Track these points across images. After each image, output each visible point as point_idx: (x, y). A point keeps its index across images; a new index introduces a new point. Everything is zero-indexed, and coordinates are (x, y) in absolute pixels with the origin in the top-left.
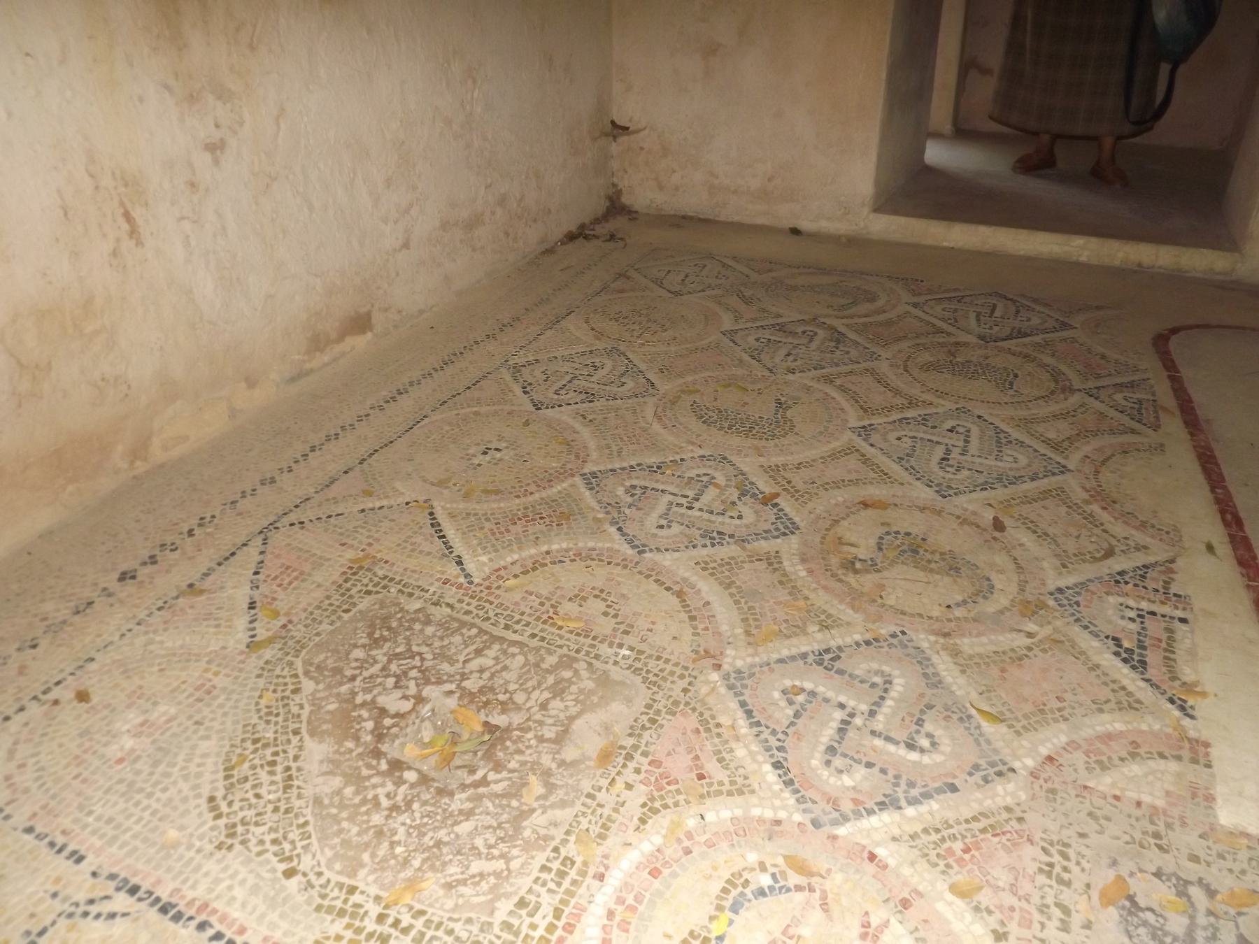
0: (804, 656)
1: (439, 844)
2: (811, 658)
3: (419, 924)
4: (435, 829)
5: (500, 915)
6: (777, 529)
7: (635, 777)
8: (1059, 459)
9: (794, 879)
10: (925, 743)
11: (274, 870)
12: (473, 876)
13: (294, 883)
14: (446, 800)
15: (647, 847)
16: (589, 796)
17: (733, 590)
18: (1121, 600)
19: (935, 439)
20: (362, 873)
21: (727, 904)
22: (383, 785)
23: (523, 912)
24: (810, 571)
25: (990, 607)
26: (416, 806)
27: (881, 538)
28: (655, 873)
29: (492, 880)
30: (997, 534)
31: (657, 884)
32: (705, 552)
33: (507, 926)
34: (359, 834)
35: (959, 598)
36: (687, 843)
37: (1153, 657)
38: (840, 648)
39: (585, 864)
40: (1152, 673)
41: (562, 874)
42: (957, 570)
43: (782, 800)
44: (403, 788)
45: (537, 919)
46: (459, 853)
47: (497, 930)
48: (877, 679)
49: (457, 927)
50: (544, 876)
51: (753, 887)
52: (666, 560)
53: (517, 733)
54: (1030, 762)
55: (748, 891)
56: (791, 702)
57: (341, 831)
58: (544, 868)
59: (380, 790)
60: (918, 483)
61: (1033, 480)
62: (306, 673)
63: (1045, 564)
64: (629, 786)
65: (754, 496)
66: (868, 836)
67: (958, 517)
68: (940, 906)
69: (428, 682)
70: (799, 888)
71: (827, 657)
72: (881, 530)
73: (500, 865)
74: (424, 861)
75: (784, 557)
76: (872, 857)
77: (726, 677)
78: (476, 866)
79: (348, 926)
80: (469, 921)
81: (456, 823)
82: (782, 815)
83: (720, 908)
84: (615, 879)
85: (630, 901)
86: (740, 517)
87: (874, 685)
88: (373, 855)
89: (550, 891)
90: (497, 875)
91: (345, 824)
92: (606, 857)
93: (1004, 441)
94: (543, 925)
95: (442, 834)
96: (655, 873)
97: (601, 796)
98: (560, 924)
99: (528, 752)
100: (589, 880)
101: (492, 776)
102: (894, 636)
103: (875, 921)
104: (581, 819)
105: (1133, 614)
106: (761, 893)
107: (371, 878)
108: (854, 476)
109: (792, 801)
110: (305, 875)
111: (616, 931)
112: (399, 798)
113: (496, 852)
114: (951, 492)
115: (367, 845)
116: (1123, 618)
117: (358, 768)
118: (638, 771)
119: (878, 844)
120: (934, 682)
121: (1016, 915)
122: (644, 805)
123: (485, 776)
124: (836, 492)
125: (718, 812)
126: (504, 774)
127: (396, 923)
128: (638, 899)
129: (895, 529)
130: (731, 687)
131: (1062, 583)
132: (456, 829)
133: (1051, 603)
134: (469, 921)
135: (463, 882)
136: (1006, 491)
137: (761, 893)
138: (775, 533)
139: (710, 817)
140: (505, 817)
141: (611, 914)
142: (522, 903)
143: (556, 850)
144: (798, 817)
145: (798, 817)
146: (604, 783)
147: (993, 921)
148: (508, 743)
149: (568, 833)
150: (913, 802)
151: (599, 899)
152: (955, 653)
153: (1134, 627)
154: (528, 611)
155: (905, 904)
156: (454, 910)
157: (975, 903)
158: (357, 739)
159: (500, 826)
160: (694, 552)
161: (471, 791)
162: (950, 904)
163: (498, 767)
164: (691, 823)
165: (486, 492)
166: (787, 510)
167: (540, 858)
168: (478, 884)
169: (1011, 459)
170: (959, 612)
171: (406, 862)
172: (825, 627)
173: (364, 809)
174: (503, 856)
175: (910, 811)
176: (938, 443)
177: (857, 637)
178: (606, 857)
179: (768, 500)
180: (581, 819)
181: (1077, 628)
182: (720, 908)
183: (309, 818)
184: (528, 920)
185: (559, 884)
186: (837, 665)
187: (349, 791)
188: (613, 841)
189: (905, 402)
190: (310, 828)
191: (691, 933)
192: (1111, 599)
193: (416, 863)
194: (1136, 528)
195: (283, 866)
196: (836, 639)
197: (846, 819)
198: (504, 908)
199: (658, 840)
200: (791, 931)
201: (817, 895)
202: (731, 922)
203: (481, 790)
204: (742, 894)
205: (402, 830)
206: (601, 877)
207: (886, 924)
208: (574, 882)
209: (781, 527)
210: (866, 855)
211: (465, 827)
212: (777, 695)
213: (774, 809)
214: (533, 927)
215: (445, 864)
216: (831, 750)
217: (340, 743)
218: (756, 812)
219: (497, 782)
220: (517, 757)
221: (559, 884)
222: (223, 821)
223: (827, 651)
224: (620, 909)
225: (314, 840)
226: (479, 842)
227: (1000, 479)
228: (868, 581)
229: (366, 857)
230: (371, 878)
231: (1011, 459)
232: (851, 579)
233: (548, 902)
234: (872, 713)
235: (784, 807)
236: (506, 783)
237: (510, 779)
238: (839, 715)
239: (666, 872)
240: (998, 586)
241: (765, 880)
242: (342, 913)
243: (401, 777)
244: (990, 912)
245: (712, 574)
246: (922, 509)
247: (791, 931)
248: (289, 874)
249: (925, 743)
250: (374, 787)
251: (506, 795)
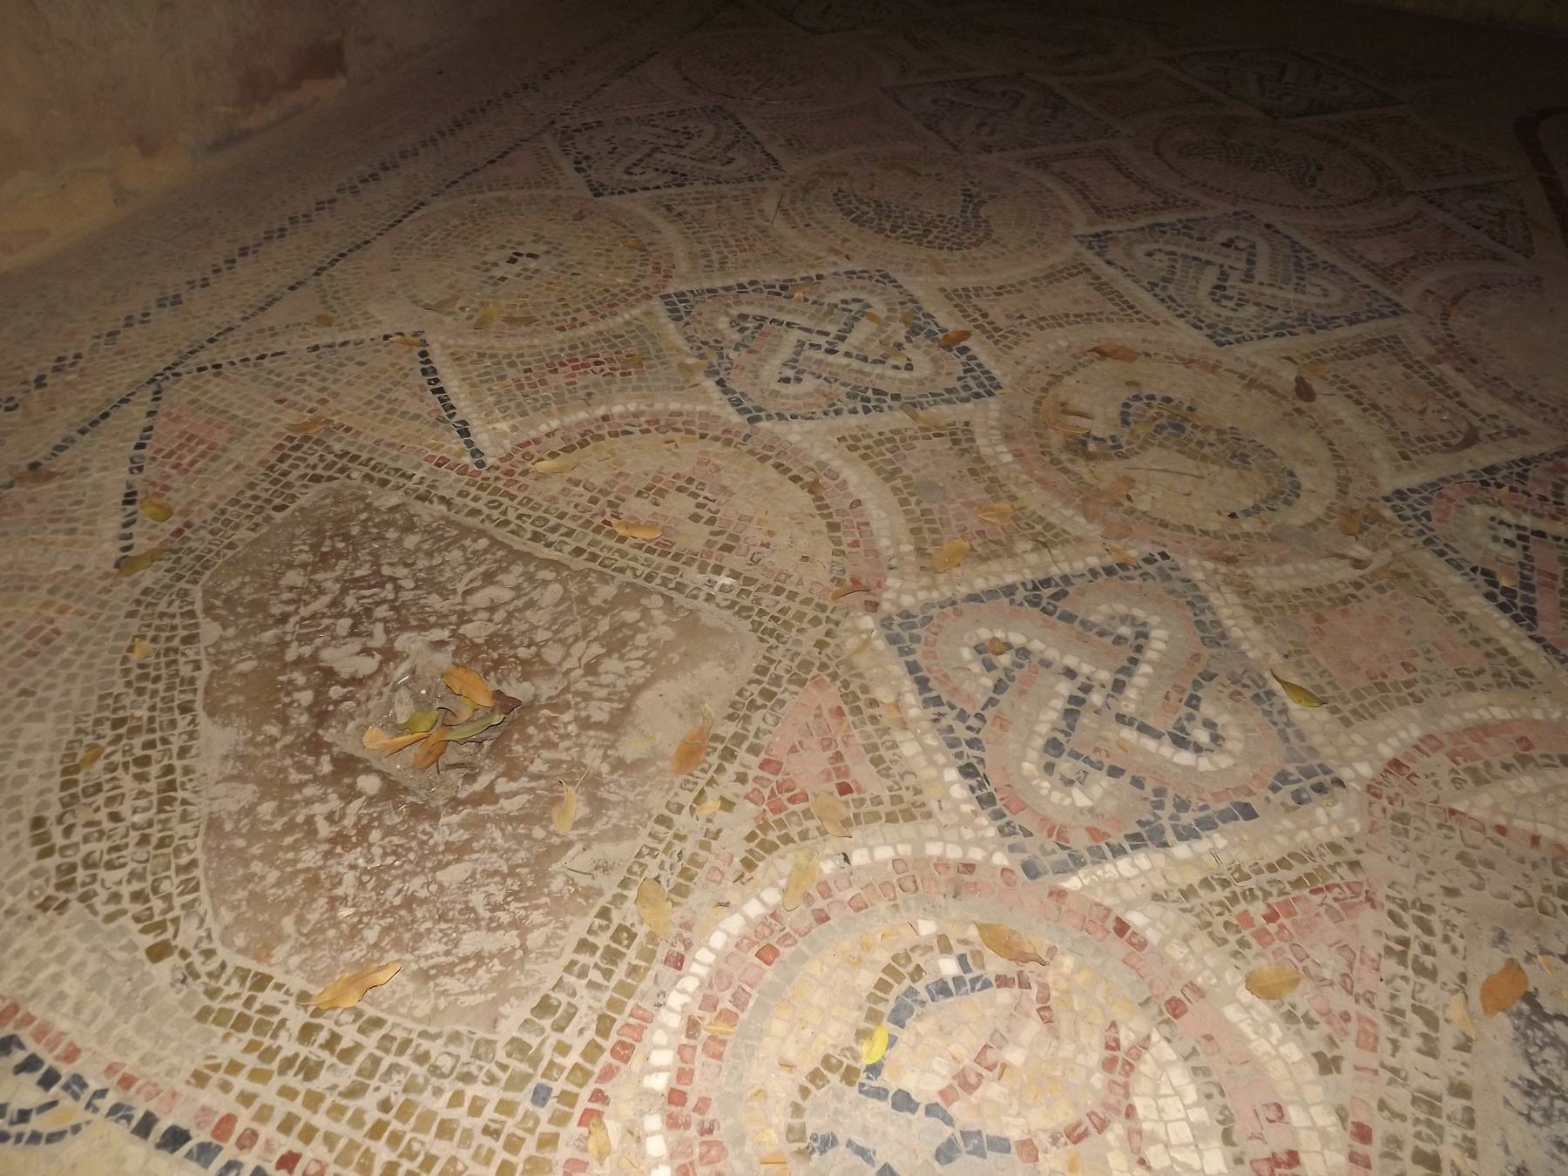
0: (1010, 590)
1: (410, 901)
2: (1020, 594)
3: (371, 1042)
4: (403, 877)
5: (509, 1028)
6: (966, 388)
7: (739, 788)
8: (1388, 293)
9: (995, 965)
10: (1202, 736)
11: (132, 947)
12: (466, 959)
13: (163, 971)
14: (426, 826)
15: (754, 909)
16: (663, 820)
17: (898, 483)
18: (1492, 511)
19: (1203, 256)
20: (280, 952)
21: (886, 1009)
22: (323, 799)
23: (547, 1023)
24: (1018, 455)
25: (1294, 518)
26: (375, 835)
27: (1126, 405)
28: (767, 955)
29: (497, 966)
30: (1302, 404)
31: (770, 973)
32: (853, 421)
33: (518, 1047)
34: (279, 884)
35: (1250, 503)
36: (820, 903)
38: (1066, 579)
39: (652, 938)
40: (1545, 628)
41: (613, 956)
42: (1244, 458)
43: (976, 829)
44: (357, 804)
45: (569, 1035)
46: (443, 917)
47: (501, 1055)
48: (1125, 630)
49: (435, 1048)
50: (584, 958)
51: (928, 979)
52: (794, 433)
53: (546, 712)
54: (1365, 770)
55: (920, 986)
56: (989, 666)
57: (249, 878)
58: (584, 946)
59: (318, 809)
60: (1180, 323)
61: (1351, 323)
62: (208, 610)
63: (1376, 454)
64: (727, 805)
65: (931, 335)
66: (1115, 891)
67: (1242, 376)
68: (1231, 1013)
69: (404, 626)
70: (1003, 981)
71: (1046, 592)
72: (1125, 394)
73: (510, 939)
74: (386, 930)
75: (978, 430)
76: (1122, 928)
77: (886, 623)
78: (471, 941)
79: (251, 1047)
80: (455, 1038)
81: (442, 866)
82: (976, 854)
83: (874, 1016)
84: (702, 962)
85: (726, 1003)
86: (909, 367)
87: (1119, 640)
88: (300, 921)
89: (592, 985)
90: (505, 956)
91: (257, 867)
92: (687, 926)
93: (1305, 263)
94: (579, 1045)
95: (416, 885)
96: (767, 955)
97: (682, 821)
98: (608, 1044)
99: (564, 744)
100: (657, 966)
101: (503, 786)
102: (1150, 560)
103: (1126, 1038)
104: (646, 860)
105: (1510, 534)
106: (942, 989)
107: (294, 961)
108: (1082, 309)
109: (991, 832)
110: (184, 954)
111: (700, 1057)
112: (349, 821)
113: (504, 917)
114: (1231, 338)
115: (291, 903)
116: (1496, 539)
117: (283, 770)
118: (742, 778)
119: (1130, 906)
120: (1215, 636)
121: (1353, 1027)
122: (751, 837)
123: (491, 786)
124: (1059, 332)
125: (871, 849)
126: (524, 782)
127: (334, 1039)
128: (739, 1000)
129: (1147, 391)
130: (893, 640)
131: (1403, 482)
132: (440, 875)
133: (1388, 513)
134: (455, 1038)
135: (447, 969)
136: (1315, 338)
137: (942, 989)
138: (963, 394)
139: (859, 858)
140: (522, 855)
141: (692, 1026)
142: (545, 1007)
143: (604, 913)
144: (1000, 859)
145: (1000, 859)
146: (687, 798)
147: (1316, 1039)
148: (531, 730)
149: (624, 884)
150: (1186, 835)
151: (675, 1000)
152: (1245, 591)
153: (1512, 554)
154: (571, 511)
155: (1176, 1008)
156: (429, 1019)
157: (1287, 1007)
158: (283, 720)
159: (512, 872)
160: (838, 421)
161: (466, 811)
162: (1247, 1008)
163: (513, 770)
164: (828, 867)
165: (511, 320)
166: (983, 358)
167: (578, 928)
168: (471, 972)
170: (1248, 525)
171: (354, 933)
172: (1042, 545)
173: (288, 840)
174: (515, 924)
175: (1181, 850)
176: (1208, 262)
177: (1093, 561)
178: (687, 926)
179: (953, 342)
180: (646, 860)
181: (1427, 555)
182: (874, 1016)
183: (199, 855)
184: (554, 1037)
185: (607, 974)
186: (1063, 606)
187: (267, 808)
188: (699, 897)
190: (197, 873)
191: (826, 1060)
192: (1477, 510)
193: (371, 935)
194: (1506, 400)
195: (149, 940)
196: (1060, 564)
197: (1078, 862)
198: (514, 1016)
199: (772, 896)
200: (991, 1057)
201: (1034, 992)
202: (892, 1041)
203: (484, 809)
204: (911, 992)
205: (350, 877)
206: (678, 962)
207: (1145, 1043)
208: (633, 970)
209: (972, 383)
210: (1110, 924)
211: (454, 874)
212: (966, 653)
213: (964, 844)
214: (563, 1049)
215: (418, 937)
216: (1054, 746)
217: (256, 728)
218: (934, 849)
219: (511, 795)
220: (545, 754)
221: (607, 974)
222: (56, 860)
223: (1047, 582)
224: (709, 1017)
225: (203, 893)
226: (477, 899)
227: (1302, 320)
228: (1107, 473)
229: (288, 923)
230: (294, 961)
231: (1317, 291)
232: (1081, 467)
233: (588, 1005)
234: (1119, 686)
235: (980, 842)
236: (523, 799)
237: (532, 790)
238: (1065, 688)
239: (785, 952)
240: (1307, 484)
241: (949, 967)
242: (242, 1023)
243: (352, 786)
244: (1311, 1023)
245: (865, 457)
247: (991, 1057)
248: (158, 953)
249: (1202, 736)
250: (309, 802)
251: (525, 818)
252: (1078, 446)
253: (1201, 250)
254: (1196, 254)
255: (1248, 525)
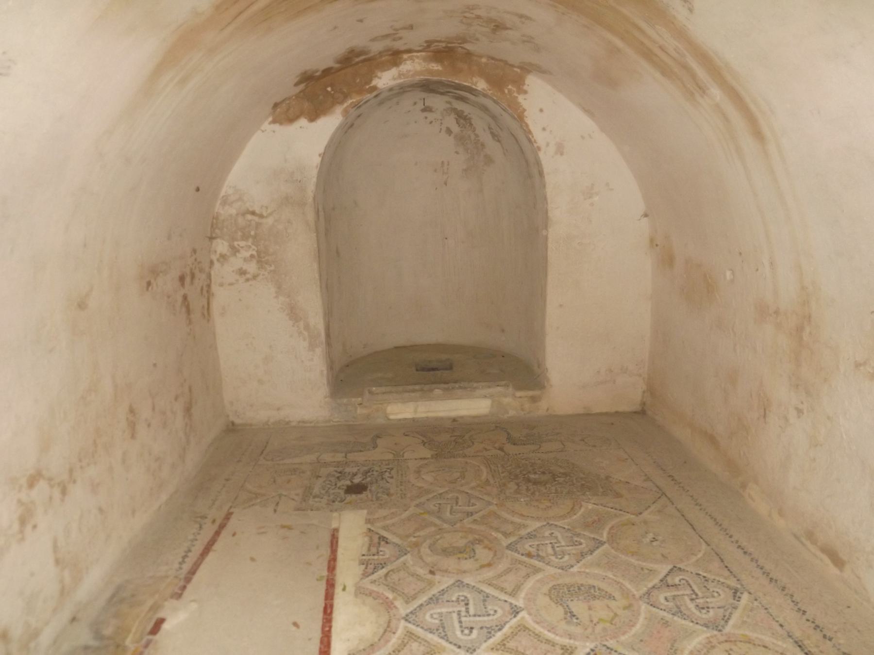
8: (410, 626)
19: (478, 619)
25: (428, 542)
37: (376, 540)
60: (473, 584)
61: (422, 605)
63: (411, 563)
72: (477, 557)
75: (503, 538)
93: (441, 630)
120: (439, 518)
131: (405, 557)
133: (409, 549)
136: (433, 593)
152: (435, 525)
153: (381, 549)
169: (435, 616)
172: (475, 520)
176: (475, 616)
189: (508, 645)
192: (387, 556)
194: (374, 591)
196: (471, 519)
227: (437, 599)
228: (471, 537)
231: (435, 616)
238: (460, 504)
246: (465, 572)
252: (480, 541)
253: (480, 621)
254: (481, 619)
255: (438, 537)
